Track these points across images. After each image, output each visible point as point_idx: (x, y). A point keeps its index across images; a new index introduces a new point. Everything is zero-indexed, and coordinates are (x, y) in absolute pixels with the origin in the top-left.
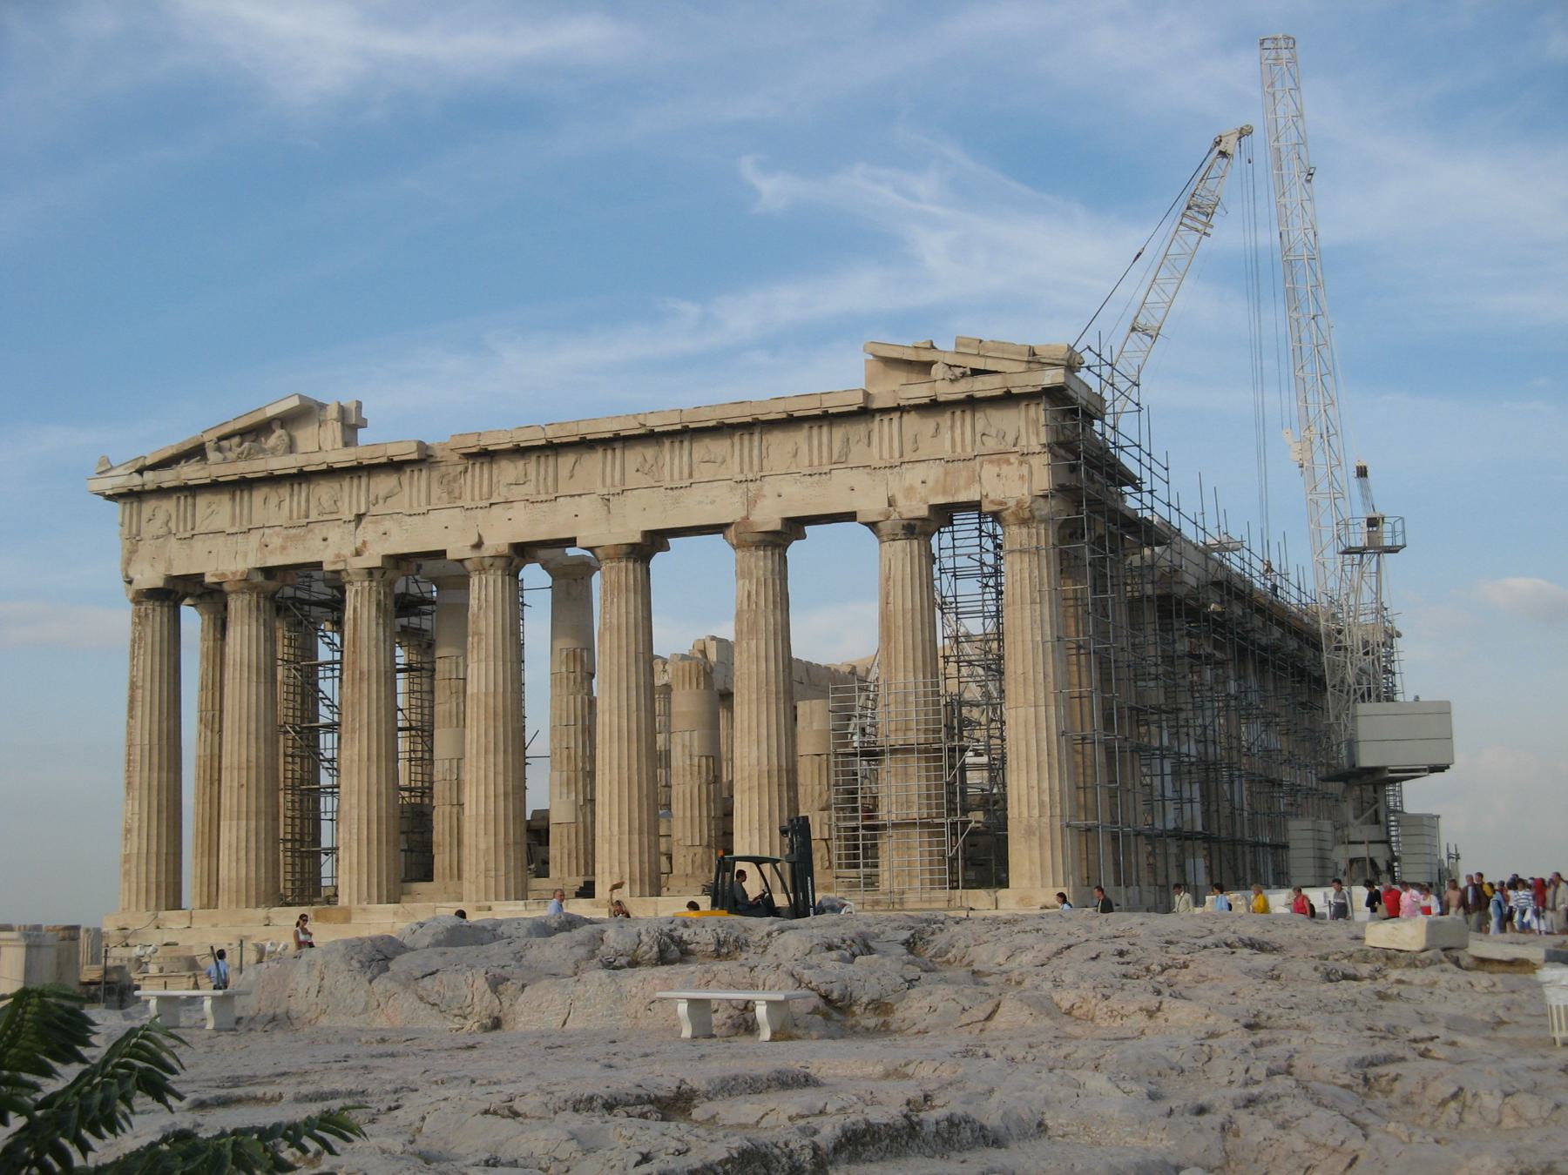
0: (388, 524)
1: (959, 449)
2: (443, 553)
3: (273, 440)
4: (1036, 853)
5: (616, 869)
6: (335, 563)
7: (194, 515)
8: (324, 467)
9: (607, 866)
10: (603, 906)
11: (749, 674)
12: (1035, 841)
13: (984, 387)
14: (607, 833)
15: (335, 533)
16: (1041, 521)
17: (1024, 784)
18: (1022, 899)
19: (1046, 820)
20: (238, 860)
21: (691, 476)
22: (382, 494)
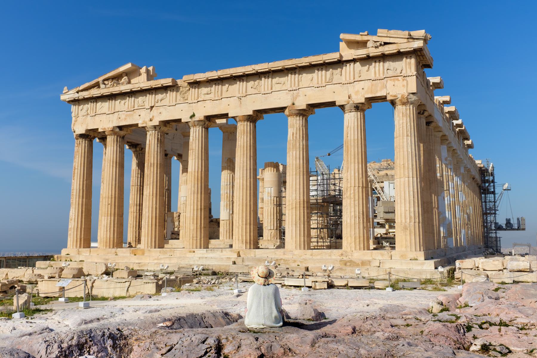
0: (161, 109)
1: (377, 75)
2: (181, 120)
3: (123, 80)
4: (408, 237)
5: (241, 238)
6: (143, 124)
7: (96, 108)
8: (139, 89)
9: (237, 237)
10: (235, 252)
11: (292, 164)
12: (408, 231)
13: (388, 50)
14: (237, 224)
15: (143, 113)
16: (412, 103)
17: (403, 209)
18: (402, 256)
19: (412, 223)
20: (107, 231)
21: (272, 89)
22: (160, 99)
